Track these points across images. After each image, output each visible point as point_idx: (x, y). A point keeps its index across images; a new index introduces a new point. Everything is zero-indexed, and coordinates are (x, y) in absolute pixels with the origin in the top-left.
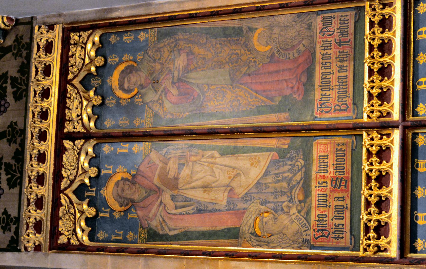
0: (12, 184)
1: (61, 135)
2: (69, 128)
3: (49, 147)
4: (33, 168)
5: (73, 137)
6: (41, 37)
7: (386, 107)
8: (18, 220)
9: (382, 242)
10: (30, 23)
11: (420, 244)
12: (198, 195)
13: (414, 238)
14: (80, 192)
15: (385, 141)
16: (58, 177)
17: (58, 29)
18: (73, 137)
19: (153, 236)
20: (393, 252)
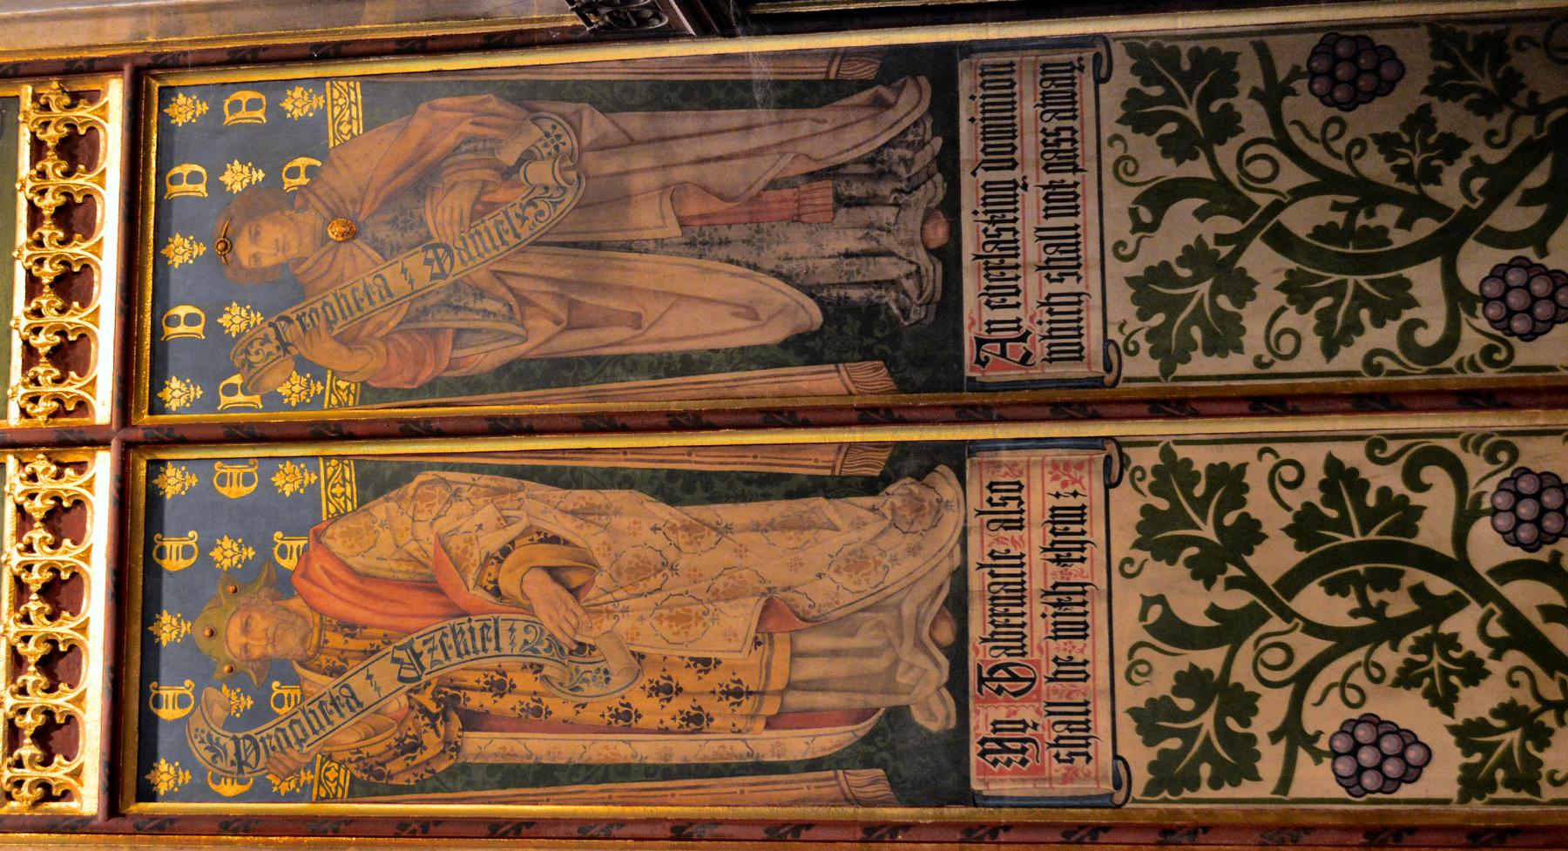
7: (73, 387)
9: (58, 772)
11: (165, 774)
13: (148, 759)
15: (71, 484)
20: (89, 800)
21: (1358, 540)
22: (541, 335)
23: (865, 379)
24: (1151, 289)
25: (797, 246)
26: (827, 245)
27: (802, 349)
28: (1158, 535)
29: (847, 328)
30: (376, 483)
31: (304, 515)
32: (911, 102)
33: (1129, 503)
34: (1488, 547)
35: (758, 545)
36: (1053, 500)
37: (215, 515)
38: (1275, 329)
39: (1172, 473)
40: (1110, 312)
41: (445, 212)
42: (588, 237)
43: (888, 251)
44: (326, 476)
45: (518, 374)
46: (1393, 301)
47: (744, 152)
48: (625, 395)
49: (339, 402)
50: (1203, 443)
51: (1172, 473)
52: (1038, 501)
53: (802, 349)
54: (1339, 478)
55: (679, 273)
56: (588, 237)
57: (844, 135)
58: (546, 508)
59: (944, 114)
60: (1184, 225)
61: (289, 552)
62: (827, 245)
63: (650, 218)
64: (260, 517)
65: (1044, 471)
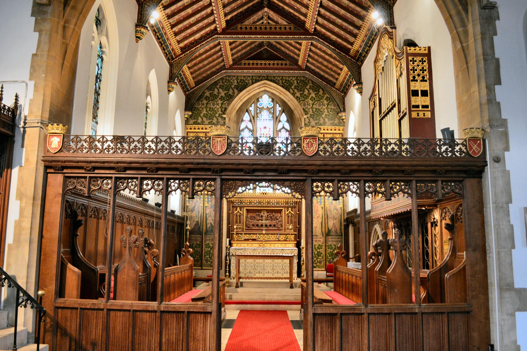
0: (316, 123)
1: (324, 133)
2: (325, 135)
6: (341, 128)
10: (344, 125)
17: (342, 132)
21: (319, 254)
22: (329, 216)
23: (327, 232)
24: (331, 245)
25: (333, 229)
26: (333, 230)
27: (328, 229)
28: (319, 245)
29: (329, 231)
30: (322, 208)
31: (321, 204)
32: (340, 234)
33: (321, 244)
34: (319, 260)
37: (321, 199)
38: (329, 251)
39: (322, 246)
40: (330, 243)
41: (335, 211)
42: (334, 218)
43: (333, 232)
44: (323, 206)
45: (327, 215)
47: (338, 226)
48: (326, 220)
49: (326, 206)
50: (323, 247)
51: (322, 246)
52: (321, 240)
53: (328, 229)
54: (322, 253)
55: (332, 223)
56: (334, 218)
57: (338, 231)
58: (321, 216)
59: (339, 236)
60: (334, 247)
61: (319, 203)
62: (333, 230)
63: (335, 221)
64: (321, 202)
65: (322, 240)
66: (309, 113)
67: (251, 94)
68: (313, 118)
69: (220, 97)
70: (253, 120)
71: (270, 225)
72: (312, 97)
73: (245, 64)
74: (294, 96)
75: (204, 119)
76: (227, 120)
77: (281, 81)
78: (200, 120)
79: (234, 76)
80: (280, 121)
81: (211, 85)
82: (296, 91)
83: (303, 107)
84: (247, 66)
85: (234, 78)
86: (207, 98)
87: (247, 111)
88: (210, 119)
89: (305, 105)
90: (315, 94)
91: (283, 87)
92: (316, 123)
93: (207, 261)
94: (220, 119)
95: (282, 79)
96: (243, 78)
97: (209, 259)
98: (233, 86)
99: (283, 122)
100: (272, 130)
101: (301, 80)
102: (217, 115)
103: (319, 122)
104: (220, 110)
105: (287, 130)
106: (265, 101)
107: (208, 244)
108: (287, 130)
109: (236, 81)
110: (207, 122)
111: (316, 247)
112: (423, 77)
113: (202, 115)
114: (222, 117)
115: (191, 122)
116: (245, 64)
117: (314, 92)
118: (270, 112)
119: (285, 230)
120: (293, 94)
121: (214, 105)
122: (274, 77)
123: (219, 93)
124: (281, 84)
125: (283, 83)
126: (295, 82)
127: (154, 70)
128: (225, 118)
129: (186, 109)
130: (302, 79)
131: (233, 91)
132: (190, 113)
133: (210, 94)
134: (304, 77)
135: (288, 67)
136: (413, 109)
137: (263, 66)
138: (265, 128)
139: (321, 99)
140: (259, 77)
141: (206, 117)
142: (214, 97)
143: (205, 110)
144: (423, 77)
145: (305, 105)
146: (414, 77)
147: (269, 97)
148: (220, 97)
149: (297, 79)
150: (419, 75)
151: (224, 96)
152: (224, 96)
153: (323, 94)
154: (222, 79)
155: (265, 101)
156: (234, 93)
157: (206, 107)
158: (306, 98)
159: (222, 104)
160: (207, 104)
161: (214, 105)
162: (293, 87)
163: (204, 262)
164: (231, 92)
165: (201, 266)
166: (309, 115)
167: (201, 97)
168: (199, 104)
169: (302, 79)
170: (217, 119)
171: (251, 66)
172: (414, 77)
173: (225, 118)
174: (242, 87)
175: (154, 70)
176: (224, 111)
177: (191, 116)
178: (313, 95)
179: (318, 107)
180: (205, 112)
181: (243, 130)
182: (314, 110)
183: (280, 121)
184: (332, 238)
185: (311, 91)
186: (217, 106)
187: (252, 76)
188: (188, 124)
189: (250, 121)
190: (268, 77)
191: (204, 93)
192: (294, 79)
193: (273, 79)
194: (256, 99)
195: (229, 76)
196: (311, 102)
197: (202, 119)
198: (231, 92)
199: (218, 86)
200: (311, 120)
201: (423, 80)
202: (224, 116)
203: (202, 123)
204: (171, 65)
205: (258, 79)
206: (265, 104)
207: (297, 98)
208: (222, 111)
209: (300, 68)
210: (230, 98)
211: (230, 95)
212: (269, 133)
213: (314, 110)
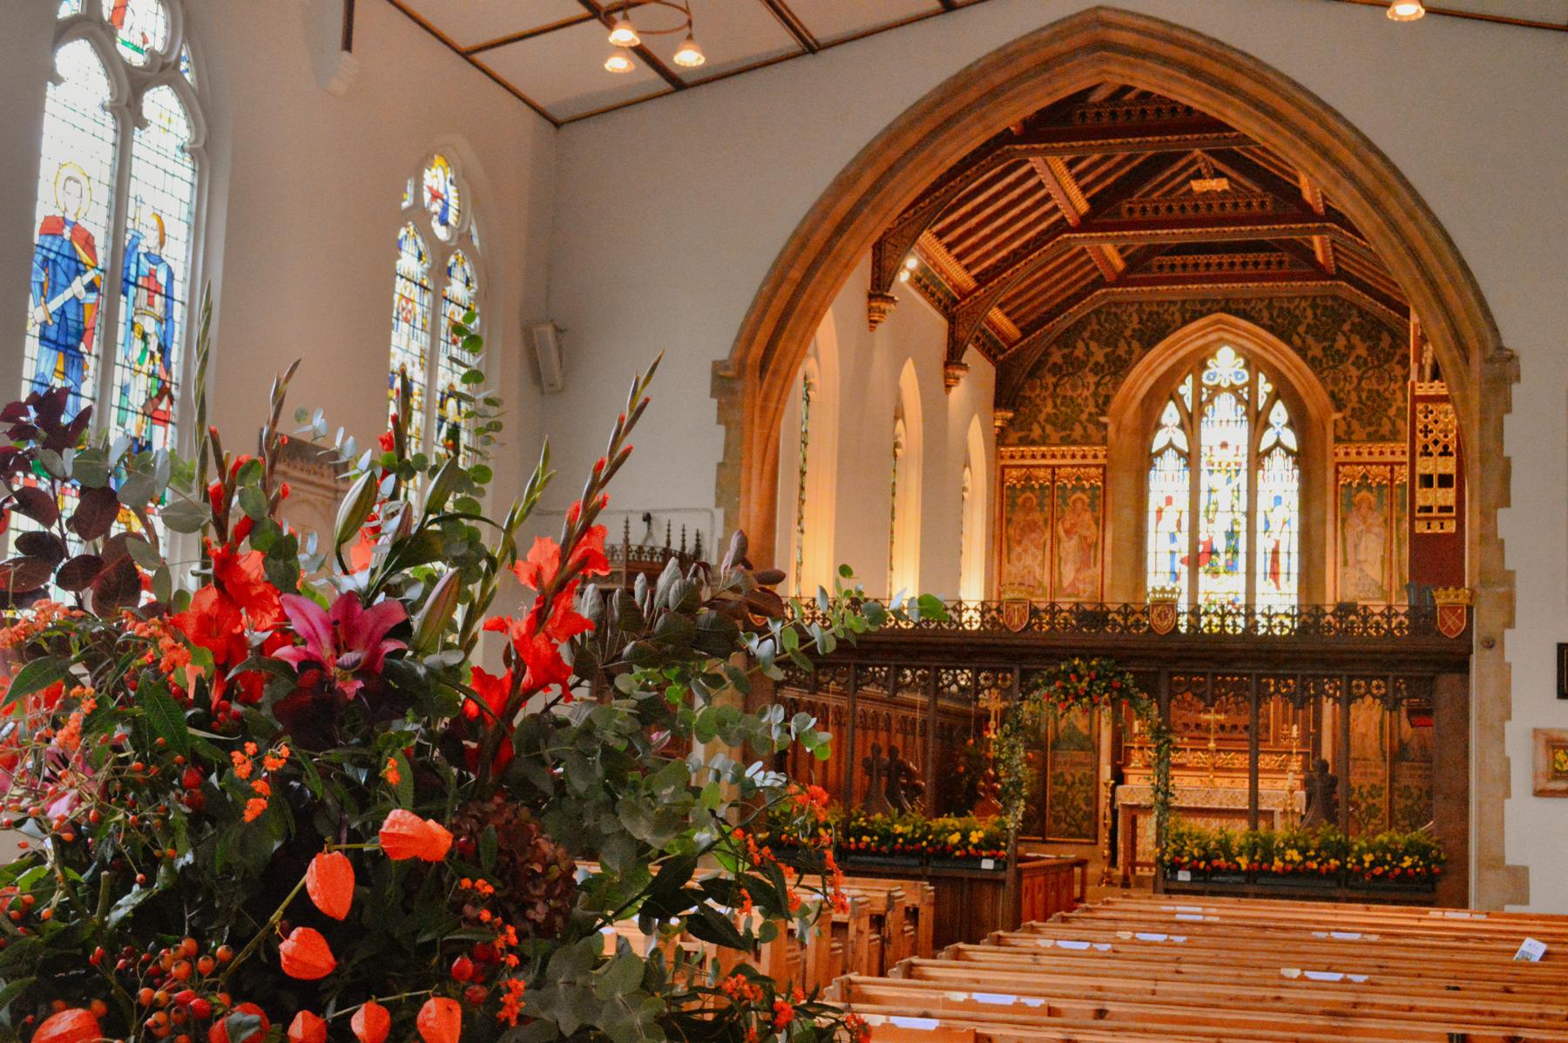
0: (1369, 435)
1: (1392, 464)
3: (1388, 458)
4: (1376, 449)
5: (1392, 471)
8: (1350, 441)
12: (1363, 544)
14: (1365, 477)
16: (1371, 464)
18: (1392, 471)
19: (1344, 520)
26: (1415, 744)
27: (1401, 741)
28: (1373, 786)
29: (1403, 746)
33: (1377, 783)
35: (1373, 732)
36: (1381, 771)
38: (1401, 803)
40: (1405, 782)
46: (1404, 818)
53: (1401, 741)
54: (1380, 810)
66: (1350, 406)
67: (1181, 354)
68: (1360, 420)
69: (1091, 364)
70: (1190, 422)
71: (1235, 727)
72: (1358, 357)
73: (1161, 267)
74: (1304, 357)
75: (1049, 428)
76: (1111, 428)
77: (1265, 314)
78: (1036, 432)
79: (1132, 303)
80: (1267, 425)
81: (1068, 330)
82: (1310, 340)
83: (1331, 387)
84: (1166, 273)
85: (1131, 309)
86: (1056, 369)
87: (1172, 397)
88: (1064, 429)
89: (1335, 381)
90: (1369, 349)
91: (1271, 329)
92: (1369, 435)
93: (1057, 820)
94: (1091, 428)
95: (1270, 307)
96: (1155, 308)
97: (1062, 814)
98: (1128, 333)
99: (1278, 428)
100: (1244, 450)
101: (1325, 307)
102: (1084, 417)
103: (1376, 431)
104: (1091, 402)
105: (1289, 452)
106: (1226, 365)
107: (1062, 774)
108: (1289, 452)
109: (1135, 318)
110: (1055, 436)
111: (1364, 790)
112: (1446, 447)
113: (1042, 417)
114: (1098, 423)
115: (1014, 436)
116: (1161, 267)
117: (1363, 340)
118: (1240, 400)
119: (1276, 739)
120: (1302, 351)
121: (1074, 387)
122: (1247, 301)
123: (1089, 354)
124: (1266, 320)
125: (1271, 318)
126: (1309, 313)
127: (910, 361)
128: (1105, 426)
129: (999, 404)
130: (1330, 303)
131: (1129, 344)
132: (1010, 415)
133: (1064, 356)
134: (1335, 298)
135: (1286, 269)
136: (1418, 515)
137: (1213, 271)
138: (1224, 445)
139: (1386, 361)
140: (1203, 302)
141: (1054, 424)
142: (1074, 366)
143: (1050, 403)
144: (1446, 447)
145: (1335, 381)
146: (1426, 447)
147: (1238, 355)
148: (1091, 364)
149: (1314, 306)
150: (1436, 442)
151: (1101, 360)
152: (1101, 360)
153: (1391, 346)
154: (1097, 312)
155: (1226, 365)
156: (1130, 352)
157: (1054, 396)
158: (1341, 362)
159: (1097, 384)
160: (1056, 386)
161: (1074, 387)
162: (1301, 329)
163: (1049, 822)
164: (1122, 350)
165: (1043, 835)
166: (1348, 412)
167: (1039, 365)
168: (1033, 389)
169: (1330, 303)
170: (1085, 429)
171: (1179, 272)
172: (1426, 447)
173: (1105, 426)
174: (1153, 334)
175: (910, 361)
176: (1103, 405)
177: (1011, 422)
178: (1362, 350)
179: (1376, 387)
180: (1049, 409)
181: (1160, 453)
182: (1364, 396)
183: (1267, 425)
184: (1413, 768)
185: (1355, 339)
186: (1084, 390)
187: (1184, 302)
188: (1003, 445)
189: (1182, 426)
190: (1227, 301)
191: (1047, 354)
192: (1303, 304)
193: (1242, 306)
194: (1198, 362)
195: (1117, 304)
196: (1354, 372)
197: (1043, 429)
198: (1122, 350)
199: (1086, 334)
200: (1355, 424)
201: (1445, 453)
202: (1103, 419)
203: (1044, 441)
204: (952, 319)
205: (1198, 307)
206: (1226, 375)
207: (1313, 363)
208: (1097, 406)
209: (1320, 272)
210: (1119, 367)
211: (1120, 357)
212: (1238, 459)
213: (1364, 396)
